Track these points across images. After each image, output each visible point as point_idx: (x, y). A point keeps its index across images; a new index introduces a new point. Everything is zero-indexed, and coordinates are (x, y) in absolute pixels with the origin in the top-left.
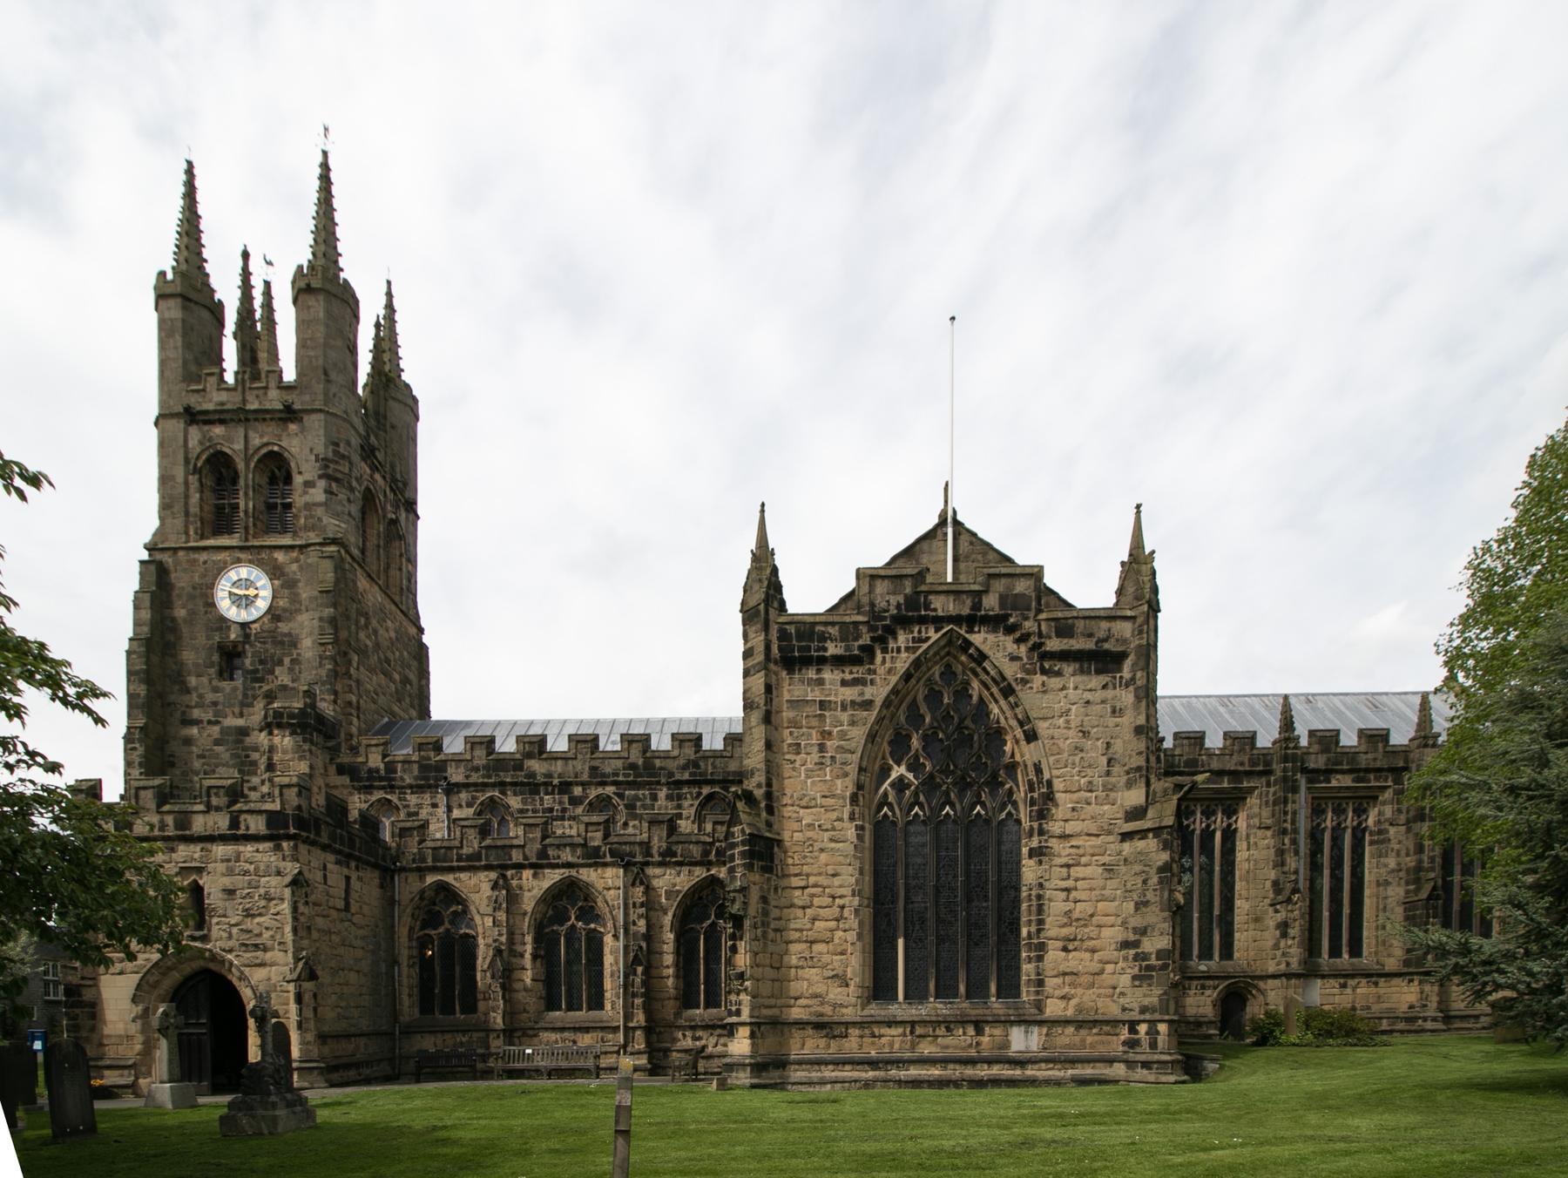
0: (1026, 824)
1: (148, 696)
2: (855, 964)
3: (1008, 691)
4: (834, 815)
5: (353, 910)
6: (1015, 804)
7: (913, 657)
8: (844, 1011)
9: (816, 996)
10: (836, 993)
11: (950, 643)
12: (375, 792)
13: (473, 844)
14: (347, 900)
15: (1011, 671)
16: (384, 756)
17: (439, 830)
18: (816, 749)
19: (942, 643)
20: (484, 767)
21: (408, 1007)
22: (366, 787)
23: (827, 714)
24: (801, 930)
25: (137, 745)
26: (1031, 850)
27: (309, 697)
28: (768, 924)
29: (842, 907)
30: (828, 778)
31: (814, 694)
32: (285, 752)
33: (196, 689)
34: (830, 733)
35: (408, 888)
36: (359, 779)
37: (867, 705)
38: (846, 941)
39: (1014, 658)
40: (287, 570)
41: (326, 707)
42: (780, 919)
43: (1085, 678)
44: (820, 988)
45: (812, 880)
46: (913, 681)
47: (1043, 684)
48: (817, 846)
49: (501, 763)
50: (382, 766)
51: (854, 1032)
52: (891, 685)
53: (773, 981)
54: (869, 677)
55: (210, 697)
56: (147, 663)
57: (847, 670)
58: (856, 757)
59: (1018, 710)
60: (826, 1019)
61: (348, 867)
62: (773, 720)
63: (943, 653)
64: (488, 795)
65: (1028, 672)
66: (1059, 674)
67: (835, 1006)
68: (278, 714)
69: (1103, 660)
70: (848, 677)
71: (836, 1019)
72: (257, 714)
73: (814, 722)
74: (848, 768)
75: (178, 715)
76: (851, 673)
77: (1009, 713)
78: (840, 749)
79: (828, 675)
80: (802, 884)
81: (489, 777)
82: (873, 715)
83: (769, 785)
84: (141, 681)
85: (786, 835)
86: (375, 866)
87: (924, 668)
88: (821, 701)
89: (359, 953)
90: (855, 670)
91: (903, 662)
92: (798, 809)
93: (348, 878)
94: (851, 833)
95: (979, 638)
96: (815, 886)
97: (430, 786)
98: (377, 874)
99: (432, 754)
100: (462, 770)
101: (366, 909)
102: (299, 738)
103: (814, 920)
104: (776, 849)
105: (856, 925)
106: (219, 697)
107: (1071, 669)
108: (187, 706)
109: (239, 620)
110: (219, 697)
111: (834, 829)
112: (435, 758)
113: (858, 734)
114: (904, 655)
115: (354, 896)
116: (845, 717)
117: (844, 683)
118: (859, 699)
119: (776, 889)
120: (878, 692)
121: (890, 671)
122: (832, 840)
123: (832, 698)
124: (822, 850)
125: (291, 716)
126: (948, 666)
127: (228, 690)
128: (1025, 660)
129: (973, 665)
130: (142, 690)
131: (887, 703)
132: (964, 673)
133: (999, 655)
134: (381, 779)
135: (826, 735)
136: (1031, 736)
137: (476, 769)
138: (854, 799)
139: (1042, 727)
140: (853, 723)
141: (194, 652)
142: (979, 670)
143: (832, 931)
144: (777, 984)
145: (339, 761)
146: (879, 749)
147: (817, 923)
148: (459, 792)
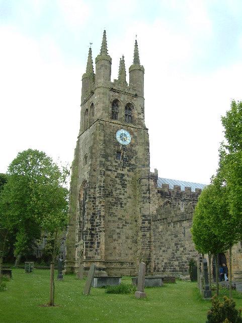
55: (114, 164)
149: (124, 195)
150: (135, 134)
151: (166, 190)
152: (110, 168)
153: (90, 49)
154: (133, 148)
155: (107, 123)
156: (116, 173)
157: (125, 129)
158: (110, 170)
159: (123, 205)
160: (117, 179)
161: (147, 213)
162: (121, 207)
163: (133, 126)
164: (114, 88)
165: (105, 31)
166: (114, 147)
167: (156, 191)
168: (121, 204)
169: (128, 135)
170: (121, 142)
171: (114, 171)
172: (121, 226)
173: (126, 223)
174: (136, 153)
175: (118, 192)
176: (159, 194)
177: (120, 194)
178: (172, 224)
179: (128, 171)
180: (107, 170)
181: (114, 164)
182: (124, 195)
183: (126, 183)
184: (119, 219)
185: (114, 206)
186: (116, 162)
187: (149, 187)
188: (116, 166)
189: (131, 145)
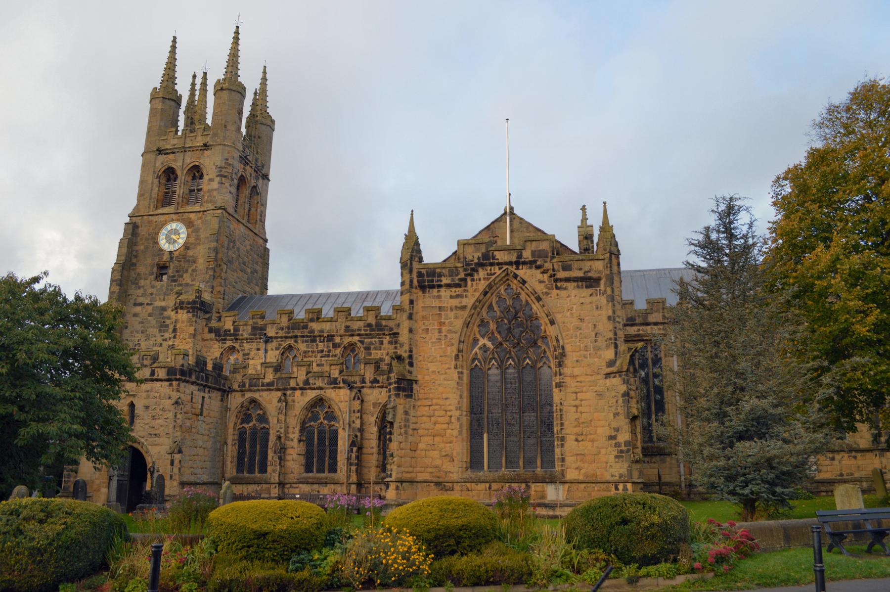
0: (554, 369)
1: (119, 292)
2: (460, 449)
3: (539, 299)
4: (447, 366)
5: (205, 414)
6: (547, 358)
7: (488, 283)
8: (451, 475)
9: (436, 467)
10: (447, 466)
11: (507, 274)
12: (227, 342)
13: (270, 377)
14: (202, 409)
15: (540, 288)
16: (234, 322)
17: (255, 365)
18: (437, 331)
19: (503, 275)
20: (286, 327)
21: (231, 469)
22: (223, 340)
23: (443, 313)
24: (428, 430)
26: (556, 383)
27: (198, 292)
28: (409, 426)
29: (451, 417)
30: (443, 346)
31: (436, 303)
32: (183, 322)
33: (143, 287)
34: (444, 323)
35: (236, 400)
36: (219, 336)
37: (464, 308)
38: (453, 436)
39: (541, 282)
40: (195, 223)
41: (207, 297)
42: (416, 423)
43: (581, 290)
44: (438, 462)
45: (434, 401)
46: (489, 295)
47: (558, 295)
48: (437, 383)
49: (295, 325)
50: (232, 328)
51: (457, 487)
52: (476, 298)
53: (412, 458)
54: (464, 294)
55: (150, 291)
56: (121, 276)
57: (453, 290)
58: (456, 337)
59: (544, 308)
60: (441, 480)
61: (204, 392)
62: (414, 317)
63: (504, 280)
64: (288, 343)
65: (549, 289)
66: (565, 289)
67: (446, 473)
68: (182, 303)
69: (590, 282)
70: (454, 294)
71: (446, 479)
72: (170, 301)
73: (436, 317)
74: (453, 341)
75: (132, 301)
76: (455, 292)
77: (541, 310)
78: (450, 331)
79: (444, 292)
80: (430, 403)
81: (289, 333)
82: (466, 313)
83: (411, 351)
84: (117, 285)
85: (419, 377)
86: (219, 390)
87: (495, 288)
88: (440, 307)
89: (206, 438)
90: (457, 289)
91: (483, 285)
92: (426, 363)
93: (203, 397)
94: (456, 376)
95: (523, 272)
96: (436, 405)
97: (256, 339)
98: (219, 393)
99: (259, 321)
100: (274, 329)
101: (212, 414)
102: (190, 315)
103: (435, 423)
104: (415, 386)
105: (458, 427)
106: (154, 291)
107: (572, 287)
108: (138, 296)
109: (169, 250)
110: (154, 291)
111: (446, 373)
112: (260, 322)
113: (459, 324)
114: (482, 282)
115: (205, 406)
116: (451, 314)
117: (451, 297)
118: (459, 305)
119: (414, 407)
120: (469, 301)
121: (475, 290)
122: (445, 380)
123: (445, 305)
124: (439, 385)
125: (189, 303)
126: (509, 285)
127: (159, 287)
128: (547, 283)
129: (521, 285)
130: (117, 289)
131: (474, 307)
132: (517, 289)
133: (533, 280)
134: (231, 335)
135: (441, 324)
136: (552, 323)
137: (282, 329)
138: (457, 357)
139: (558, 317)
140: (456, 317)
141: (145, 267)
142: (524, 287)
143: (445, 430)
144: (414, 460)
145: (210, 325)
146: (472, 329)
147: (437, 425)
148: (272, 342)
149: (161, 345)
152: (141, 300)
154: (190, 253)
155: (145, 217)
156: (150, 308)
157: (178, 220)
158: (141, 304)
171: (148, 304)
174: (194, 262)
182: (161, 345)
186: (153, 287)
188: (152, 294)
189: (186, 246)
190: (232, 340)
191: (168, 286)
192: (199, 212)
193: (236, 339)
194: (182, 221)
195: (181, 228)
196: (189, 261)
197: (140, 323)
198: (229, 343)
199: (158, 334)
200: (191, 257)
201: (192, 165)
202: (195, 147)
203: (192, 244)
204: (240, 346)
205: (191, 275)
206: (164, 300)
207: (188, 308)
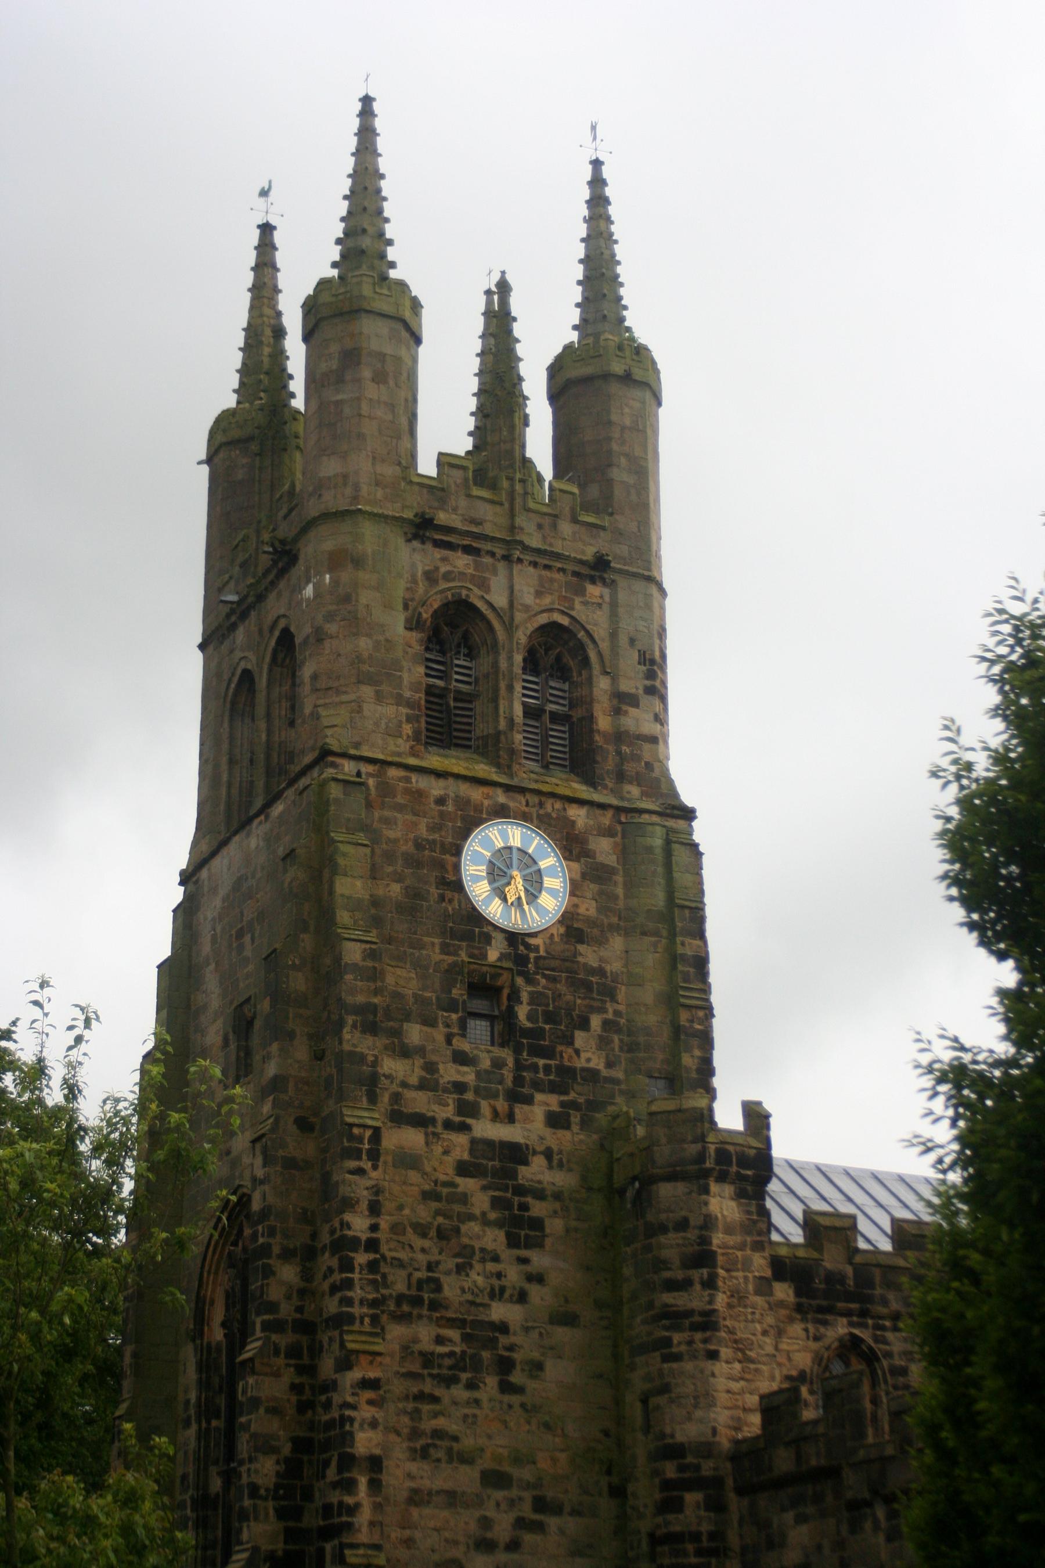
25: (367, 1165)
33: (421, 1051)
50: (849, 1270)
55: (450, 1072)
106: (468, 1075)
110: (468, 1075)
127: (486, 1063)
150: (604, 849)
151: (832, 1260)
152: (419, 1102)
153: (266, 229)
155: (393, 772)
156: (461, 1140)
157: (525, 817)
158: (420, 1121)
159: (517, 1377)
160: (468, 1184)
161: (687, 1432)
162: (506, 1387)
163: (581, 790)
164: (442, 518)
165: (367, 101)
166: (445, 949)
167: (760, 1263)
168: (505, 1366)
169: (549, 861)
170: (494, 910)
171: (448, 1125)
172: (503, 1529)
173: (541, 1505)
174: (611, 994)
175: (477, 1278)
176: (783, 1291)
177: (497, 1294)
178: (880, 1512)
179: (555, 1121)
180: (399, 1118)
181: (450, 1072)
182: (522, 1297)
183: (538, 1209)
184: (495, 1479)
185: (450, 1381)
187: (705, 1241)
188: (460, 1087)
190: (848, 1314)
191: (519, 1066)
192: (602, 806)
193: (864, 1313)
194: (545, 823)
195: (487, 843)
196: (588, 986)
197: (428, 1196)
198: (840, 1328)
199: (507, 1254)
200: (593, 971)
201: (543, 619)
202: (558, 556)
203: (592, 923)
204: (876, 1339)
205: (603, 1042)
206: (511, 1119)
207: (745, 1178)
